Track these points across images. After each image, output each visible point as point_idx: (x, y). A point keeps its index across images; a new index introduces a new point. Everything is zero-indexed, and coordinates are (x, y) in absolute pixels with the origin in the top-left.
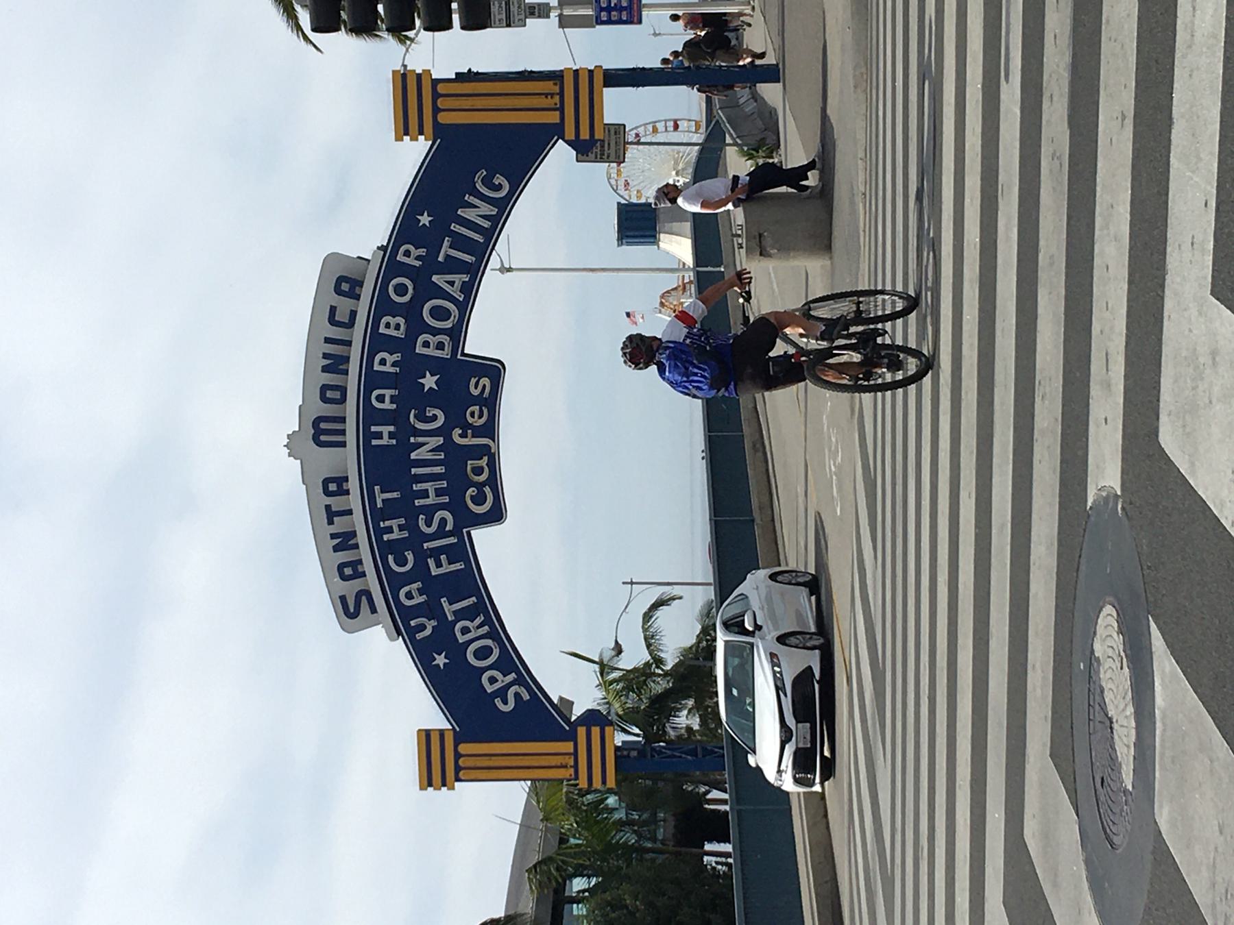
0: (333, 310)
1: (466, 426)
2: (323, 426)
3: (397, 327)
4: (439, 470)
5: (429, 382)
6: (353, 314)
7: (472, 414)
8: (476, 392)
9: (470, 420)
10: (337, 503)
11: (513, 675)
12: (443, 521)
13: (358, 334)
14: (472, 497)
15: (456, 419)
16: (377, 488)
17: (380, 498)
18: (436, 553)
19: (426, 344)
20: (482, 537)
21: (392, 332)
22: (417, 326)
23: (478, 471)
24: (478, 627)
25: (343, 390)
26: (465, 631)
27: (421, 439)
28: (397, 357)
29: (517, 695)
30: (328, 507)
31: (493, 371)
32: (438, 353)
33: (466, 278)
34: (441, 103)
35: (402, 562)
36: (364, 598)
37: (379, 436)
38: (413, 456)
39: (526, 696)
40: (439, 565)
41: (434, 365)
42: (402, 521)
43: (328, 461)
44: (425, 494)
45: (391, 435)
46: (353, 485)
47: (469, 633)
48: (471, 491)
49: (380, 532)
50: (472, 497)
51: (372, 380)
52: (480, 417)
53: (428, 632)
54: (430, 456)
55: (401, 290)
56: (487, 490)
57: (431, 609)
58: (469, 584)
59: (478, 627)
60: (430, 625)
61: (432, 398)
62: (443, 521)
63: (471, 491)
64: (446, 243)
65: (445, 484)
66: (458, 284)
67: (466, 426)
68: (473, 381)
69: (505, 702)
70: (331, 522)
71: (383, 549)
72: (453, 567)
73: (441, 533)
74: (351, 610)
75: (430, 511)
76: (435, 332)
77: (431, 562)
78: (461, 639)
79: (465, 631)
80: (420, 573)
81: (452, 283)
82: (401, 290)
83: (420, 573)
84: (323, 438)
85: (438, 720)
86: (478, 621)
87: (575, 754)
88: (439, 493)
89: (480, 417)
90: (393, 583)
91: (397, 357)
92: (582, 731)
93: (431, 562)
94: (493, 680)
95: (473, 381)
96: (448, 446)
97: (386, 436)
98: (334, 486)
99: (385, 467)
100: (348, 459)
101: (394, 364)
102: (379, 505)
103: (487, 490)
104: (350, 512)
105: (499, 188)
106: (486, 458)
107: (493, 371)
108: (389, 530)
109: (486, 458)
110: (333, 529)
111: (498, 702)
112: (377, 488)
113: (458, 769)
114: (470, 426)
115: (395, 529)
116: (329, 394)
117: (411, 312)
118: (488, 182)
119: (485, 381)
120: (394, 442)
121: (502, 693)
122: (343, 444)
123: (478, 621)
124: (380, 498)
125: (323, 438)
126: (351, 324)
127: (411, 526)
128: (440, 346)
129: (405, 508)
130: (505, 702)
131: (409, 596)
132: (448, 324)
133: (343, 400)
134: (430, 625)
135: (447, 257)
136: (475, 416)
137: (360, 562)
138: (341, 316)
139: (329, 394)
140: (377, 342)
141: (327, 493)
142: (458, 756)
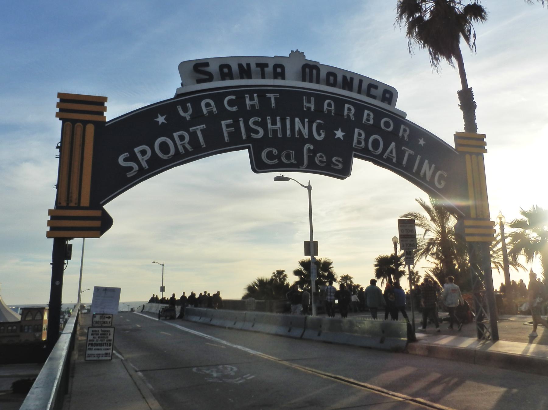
0: (376, 87)
2: (315, 72)
3: (368, 120)
4: (288, 132)
5: (339, 134)
6: (374, 97)
7: (321, 157)
8: (334, 159)
9: (318, 155)
10: (269, 70)
11: (147, 167)
13: (363, 98)
14: (272, 151)
15: (319, 146)
16: (278, 95)
17: (272, 96)
18: (236, 124)
19: (360, 134)
20: (243, 156)
21: (365, 117)
22: (369, 130)
23: (288, 157)
24: (184, 147)
25: (334, 85)
26: (182, 138)
27: (306, 125)
28: (352, 118)
29: (131, 168)
30: (266, 65)
31: (343, 172)
32: (355, 140)
33: (394, 160)
34: (474, 156)
35: (231, 103)
36: (207, 77)
37: (309, 101)
38: (297, 120)
39: (130, 175)
40: (228, 126)
41: (349, 136)
42: (257, 107)
43: (292, 70)
44: (274, 123)
45: (309, 108)
46: (279, 82)
47: (179, 139)
48: (275, 152)
49: (251, 93)
50: (271, 152)
51: (340, 102)
52: (321, 162)
53: (182, 113)
54: (297, 129)
55: (387, 124)
56: (276, 161)
57: (198, 117)
58: (215, 145)
59: (184, 147)
60: (187, 116)
61: (330, 135)
62: (257, 132)
63: (275, 152)
64: (412, 152)
65: (280, 135)
68: (340, 159)
69: (125, 160)
70: (258, 65)
71: (240, 94)
72: (226, 134)
73: (249, 130)
74: (198, 70)
77: (230, 121)
78: (176, 135)
79: (182, 138)
80: (223, 114)
81: (391, 152)
82: (387, 124)
83: (223, 114)
85: (113, 112)
86: (189, 147)
87: (79, 207)
88: (275, 132)
90: (218, 96)
91: (352, 118)
92: (98, 213)
93: (230, 121)
94: (143, 153)
95: (340, 159)
96: (302, 141)
97: (308, 105)
98: (279, 69)
99: (290, 103)
100: (292, 81)
101: (348, 116)
102: (268, 95)
103: (276, 161)
104: (263, 77)
105: (440, 184)
106: (295, 162)
107: (343, 172)
108: (252, 99)
109: (295, 162)
110: (253, 66)
111: (126, 154)
112: (278, 95)
113: (74, 122)
114: (315, 155)
115: (252, 103)
116: (332, 78)
117: (375, 129)
119: (340, 166)
120: (305, 109)
121: (133, 158)
122: (304, 80)
123: (189, 147)
124: (272, 96)
125: (307, 70)
126: (369, 95)
127: (253, 112)
128: (359, 142)
129: (264, 110)
130: (125, 160)
131: (208, 105)
132: (370, 148)
133: (328, 84)
134: (187, 116)
135: (404, 152)
136: (319, 158)
137: (232, 78)
138: (373, 91)
139: (332, 78)
140: (360, 107)
141: (276, 66)
142: (85, 123)
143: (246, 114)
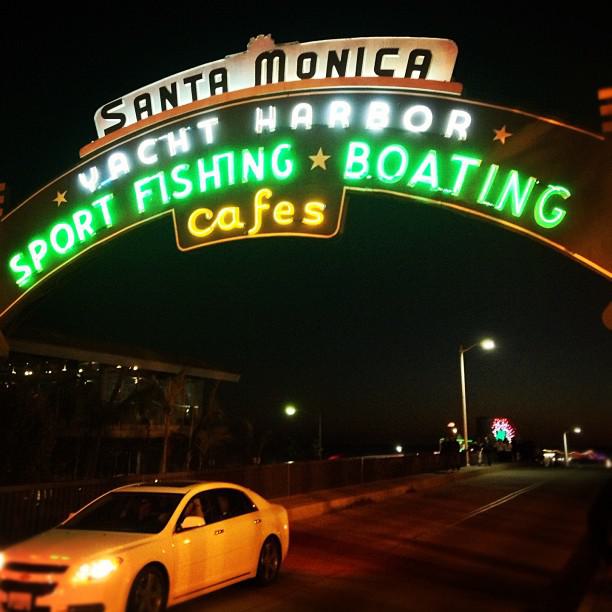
1: (273, 202)
2: (276, 59)
7: (285, 208)
12: (181, 188)
18: (155, 186)
22: (378, 142)
26: (83, 219)
40: (143, 188)
48: (209, 214)
52: (284, 217)
62: (181, 188)
63: (209, 214)
64: (476, 162)
66: (424, 179)
67: (273, 202)
69: (18, 264)
75: (192, 174)
76: (372, 160)
81: (427, 172)
84: (265, 61)
89: (284, 217)
114: (273, 206)
118: (555, 201)
125: (265, 61)
143: (166, 162)
